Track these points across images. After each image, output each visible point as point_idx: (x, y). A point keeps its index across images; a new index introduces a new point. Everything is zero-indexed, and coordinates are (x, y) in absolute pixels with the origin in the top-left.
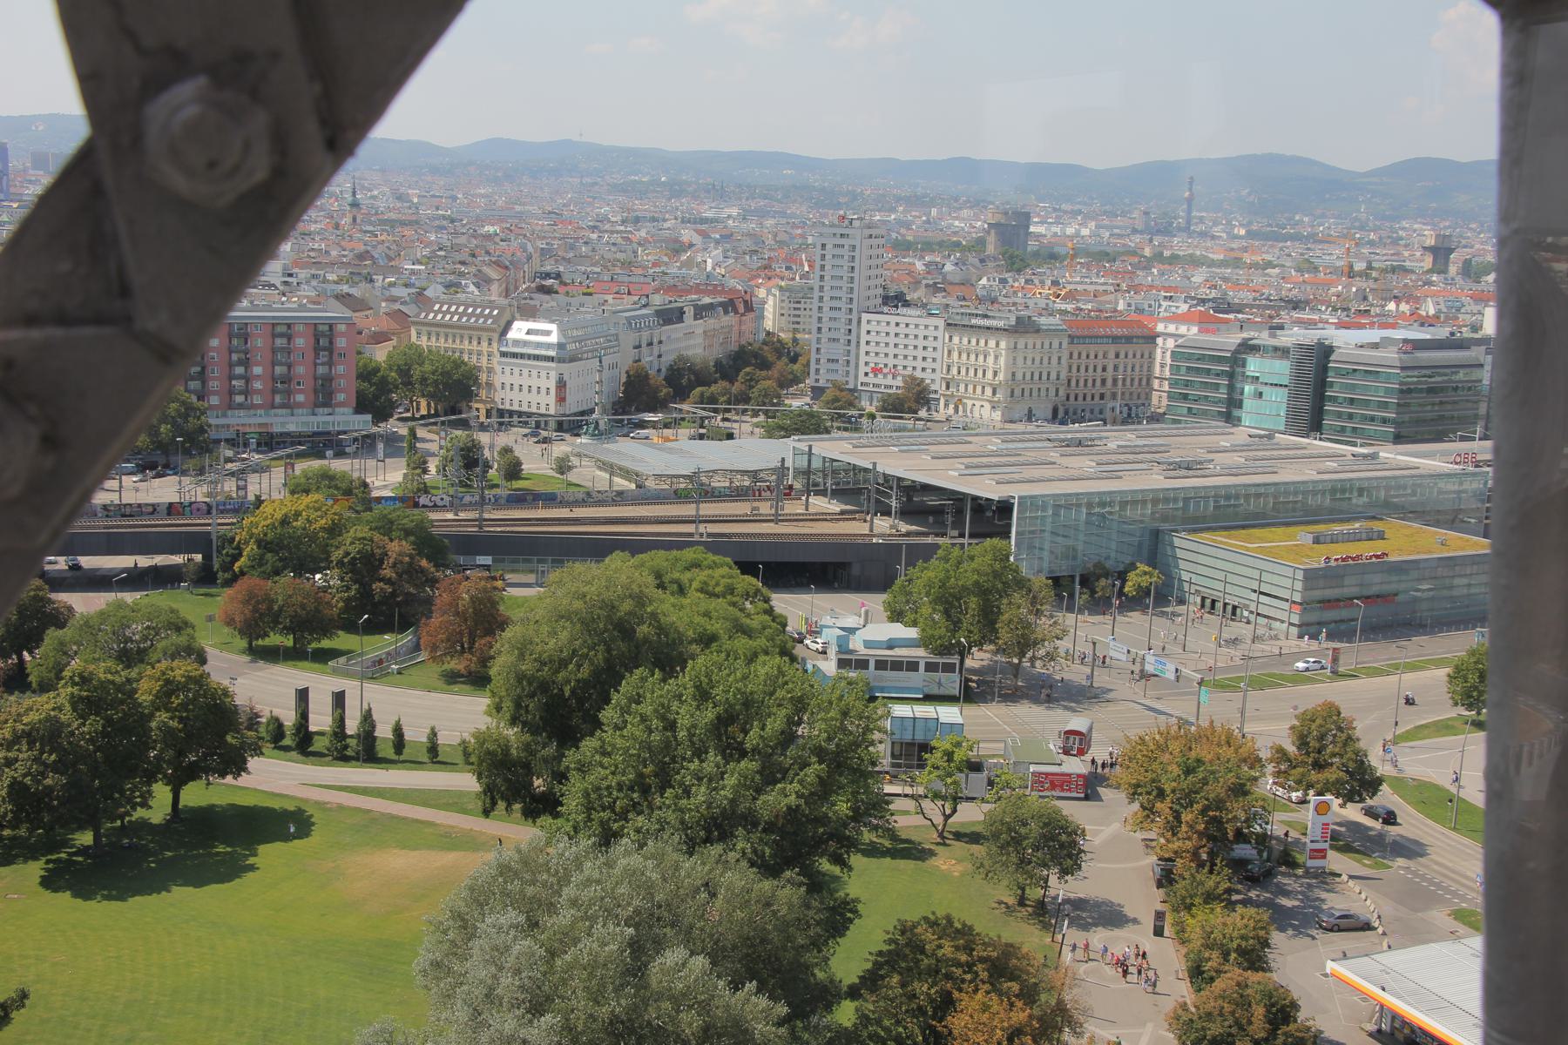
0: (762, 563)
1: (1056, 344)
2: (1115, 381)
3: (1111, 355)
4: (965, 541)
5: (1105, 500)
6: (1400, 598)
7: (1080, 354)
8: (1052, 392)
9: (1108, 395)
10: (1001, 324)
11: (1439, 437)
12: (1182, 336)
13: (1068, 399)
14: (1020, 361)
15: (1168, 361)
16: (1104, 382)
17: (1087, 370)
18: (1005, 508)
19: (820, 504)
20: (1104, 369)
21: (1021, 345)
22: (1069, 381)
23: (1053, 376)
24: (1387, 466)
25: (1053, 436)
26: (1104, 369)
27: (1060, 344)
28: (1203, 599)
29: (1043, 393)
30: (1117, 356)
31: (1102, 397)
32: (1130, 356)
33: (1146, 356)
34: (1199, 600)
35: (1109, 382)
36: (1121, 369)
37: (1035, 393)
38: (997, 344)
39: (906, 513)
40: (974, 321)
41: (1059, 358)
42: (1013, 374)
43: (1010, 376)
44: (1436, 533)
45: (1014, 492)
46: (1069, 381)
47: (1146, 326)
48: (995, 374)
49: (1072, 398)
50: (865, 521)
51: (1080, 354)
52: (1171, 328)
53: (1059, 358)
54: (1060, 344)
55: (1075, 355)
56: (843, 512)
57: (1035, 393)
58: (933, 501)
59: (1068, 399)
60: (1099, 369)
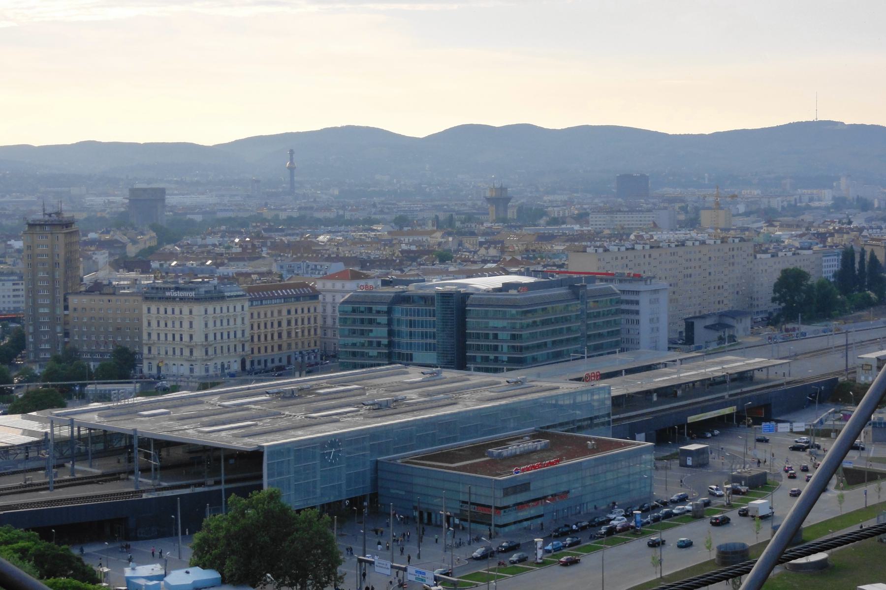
0: (53, 527)
1: (239, 308)
2: (289, 334)
3: (284, 312)
4: (223, 487)
5: (333, 442)
6: (570, 496)
7: (259, 314)
8: (239, 349)
9: (285, 346)
10: (192, 294)
11: (557, 357)
12: (348, 292)
13: (252, 352)
14: (211, 324)
15: (338, 314)
16: (280, 336)
17: (266, 327)
18: (256, 455)
19: (83, 468)
20: (280, 324)
21: (210, 310)
22: (252, 338)
23: (239, 334)
24: (534, 389)
25: (268, 390)
26: (280, 324)
27: (243, 307)
28: (421, 514)
29: (232, 349)
30: (289, 312)
31: (280, 347)
32: (299, 311)
33: (312, 310)
34: (416, 514)
35: (285, 335)
36: (293, 322)
37: (225, 350)
38: (191, 312)
39: (168, 468)
40: (168, 294)
41: (243, 319)
42: (206, 337)
43: (203, 339)
44: (590, 440)
45: (266, 442)
46: (252, 338)
47: (307, 286)
48: (191, 337)
49: (256, 351)
50: (128, 479)
51: (259, 314)
52: (329, 285)
53: (243, 319)
54: (243, 307)
55: (255, 316)
56: (103, 475)
57: (225, 350)
58: (177, 454)
59: (252, 352)
60: (276, 325)
